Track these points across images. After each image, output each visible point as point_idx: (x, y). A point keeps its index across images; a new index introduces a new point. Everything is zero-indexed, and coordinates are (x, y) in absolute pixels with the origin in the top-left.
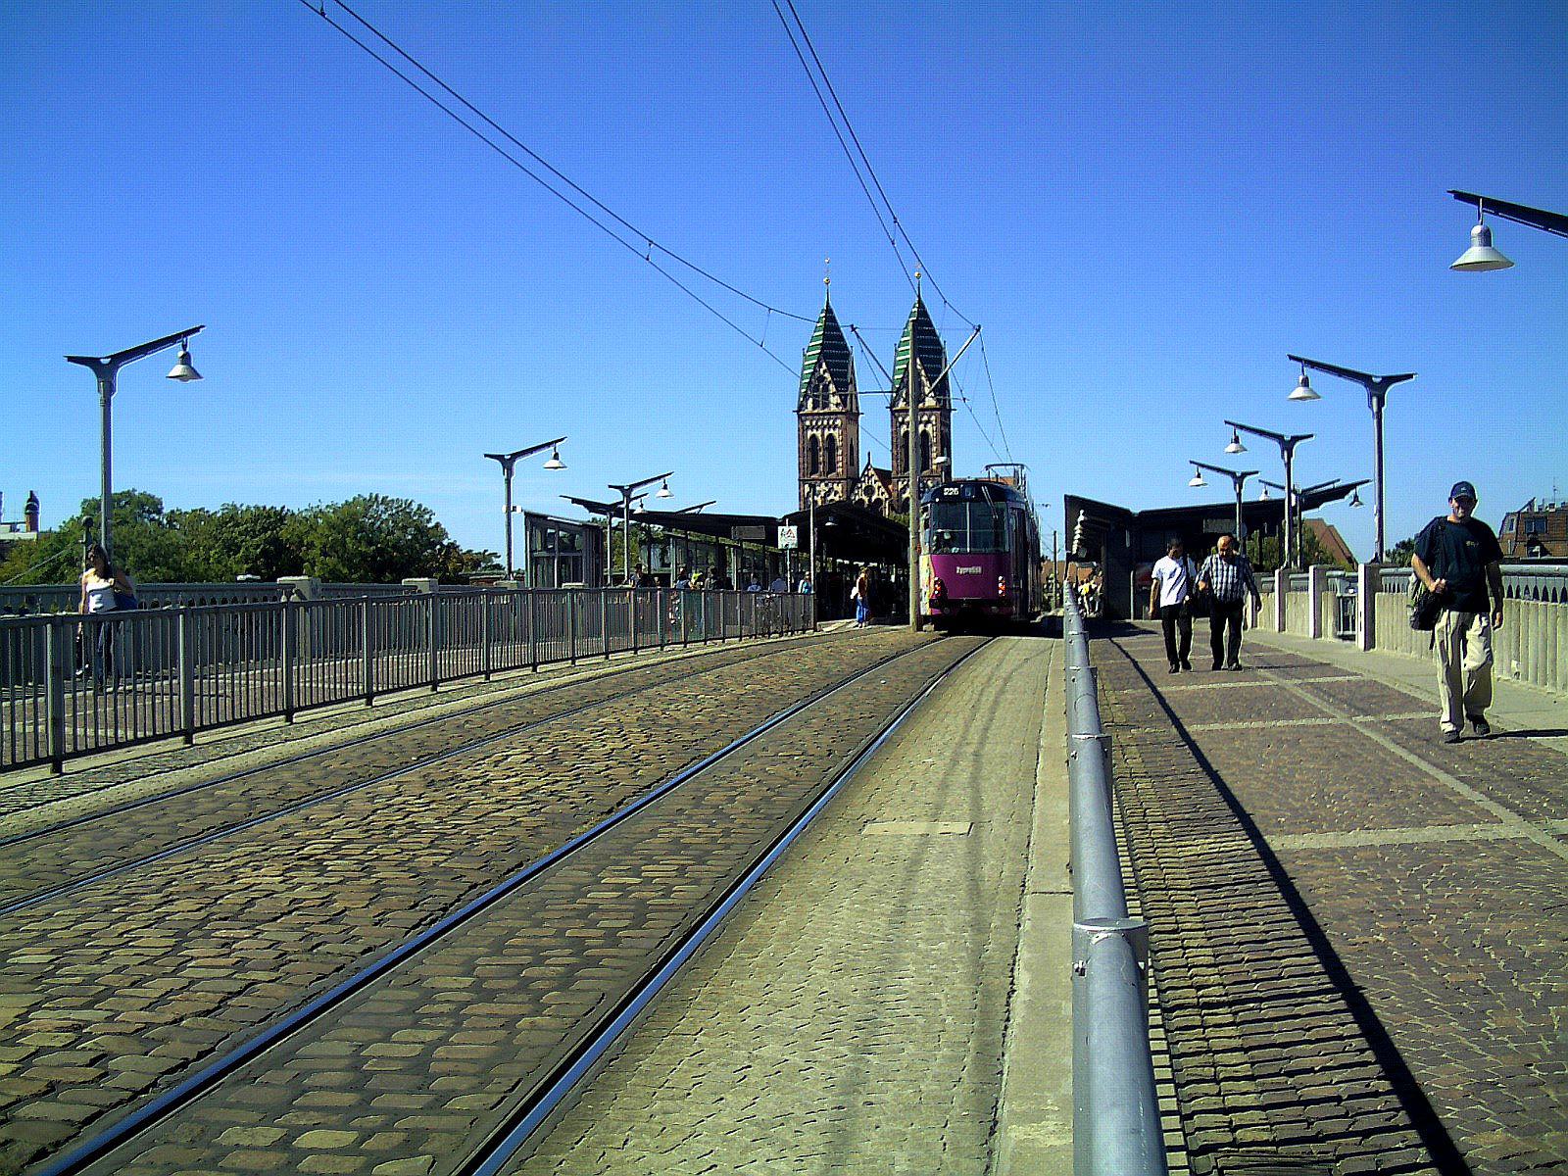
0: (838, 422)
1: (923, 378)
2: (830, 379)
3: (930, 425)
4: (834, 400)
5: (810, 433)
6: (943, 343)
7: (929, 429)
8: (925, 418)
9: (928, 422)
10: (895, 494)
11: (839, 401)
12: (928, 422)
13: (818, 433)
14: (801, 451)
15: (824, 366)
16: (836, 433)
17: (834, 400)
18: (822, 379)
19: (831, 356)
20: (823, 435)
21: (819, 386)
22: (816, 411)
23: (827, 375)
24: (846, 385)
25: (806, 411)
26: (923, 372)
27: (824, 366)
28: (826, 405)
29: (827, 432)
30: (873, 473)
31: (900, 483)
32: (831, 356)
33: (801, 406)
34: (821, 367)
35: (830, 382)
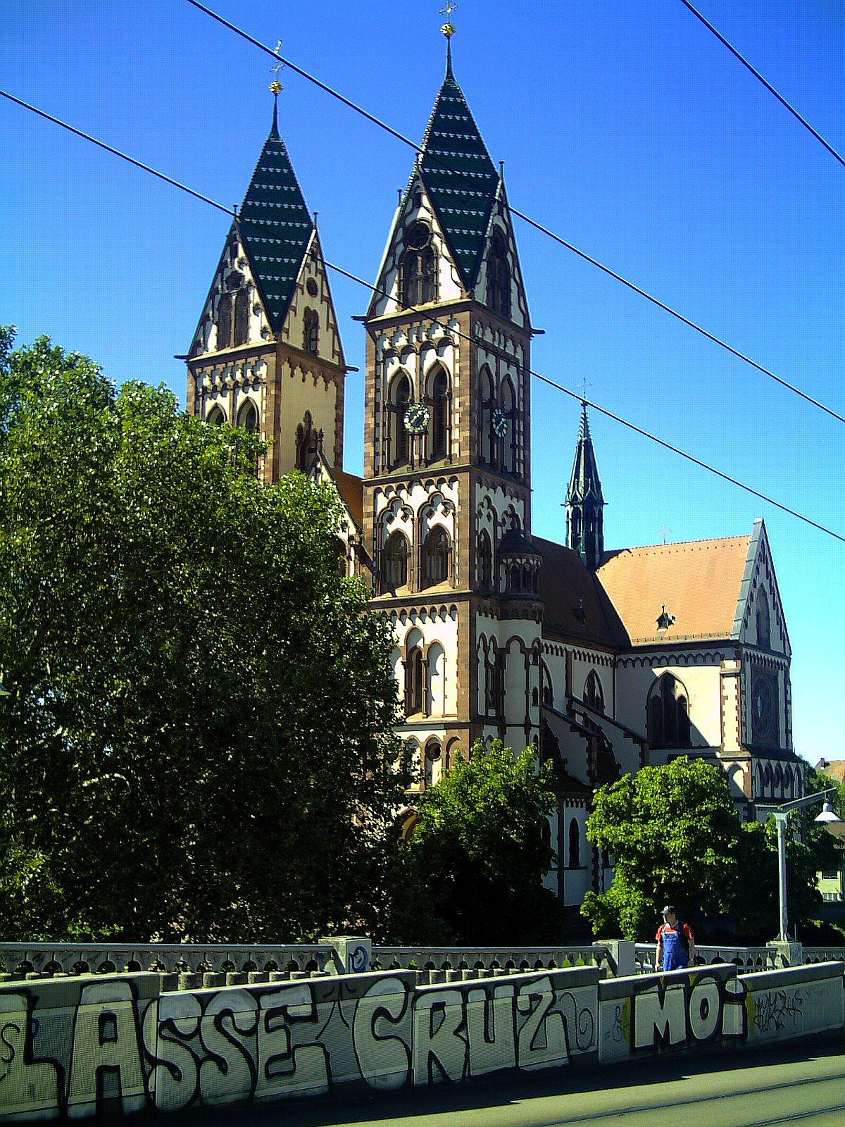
0: (263, 372)
3: (449, 349)
4: (257, 322)
6: (498, 171)
9: (445, 342)
10: (368, 523)
11: (265, 323)
12: (445, 342)
13: (224, 402)
15: (241, 253)
16: (257, 396)
17: (257, 322)
21: (228, 296)
25: (205, 355)
26: (436, 227)
27: (241, 253)
28: (242, 336)
29: (241, 397)
31: (380, 496)
33: (197, 345)
34: (234, 254)
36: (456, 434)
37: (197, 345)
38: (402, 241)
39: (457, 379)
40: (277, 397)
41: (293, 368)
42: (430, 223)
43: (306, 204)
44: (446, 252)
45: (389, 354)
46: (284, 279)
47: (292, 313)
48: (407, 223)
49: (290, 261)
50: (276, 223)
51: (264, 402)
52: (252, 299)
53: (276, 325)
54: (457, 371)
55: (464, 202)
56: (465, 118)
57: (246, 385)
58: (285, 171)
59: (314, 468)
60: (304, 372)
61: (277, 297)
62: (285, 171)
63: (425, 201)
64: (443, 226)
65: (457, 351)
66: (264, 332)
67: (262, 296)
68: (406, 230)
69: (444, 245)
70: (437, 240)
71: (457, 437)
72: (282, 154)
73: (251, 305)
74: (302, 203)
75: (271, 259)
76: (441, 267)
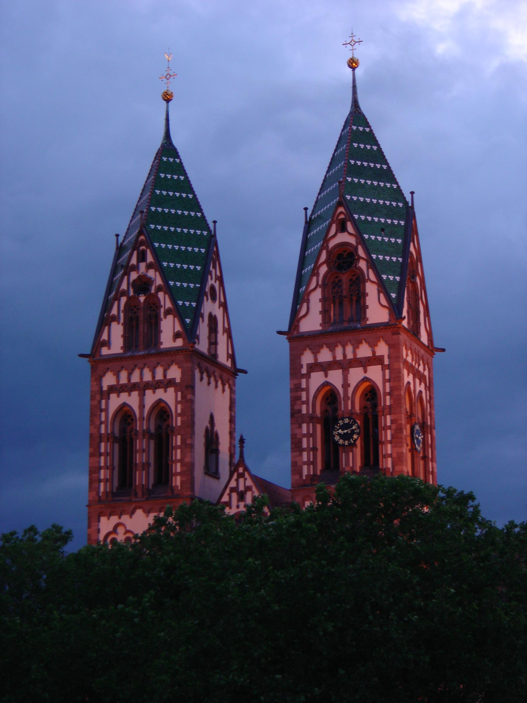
1: (362, 264)
2: (159, 281)
5: (115, 402)
6: (408, 198)
7: (375, 373)
8: (364, 351)
9: (376, 360)
11: (178, 328)
13: (132, 400)
14: (95, 439)
15: (150, 258)
16: (169, 396)
17: (169, 326)
18: (143, 285)
19: (166, 237)
20: (142, 406)
22: (129, 354)
23: (151, 273)
24: (199, 296)
26: (361, 252)
27: (150, 258)
29: (151, 398)
30: (249, 483)
32: (166, 237)
33: (99, 343)
34: (142, 257)
35: (159, 289)
36: (389, 449)
37: (99, 343)
38: (326, 262)
39: (388, 397)
40: (192, 402)
41: (202, 373)
42: (356, 249)
43: (204, 211)
44: (372, 277)
45: (314, 367)
46: (192, 286)
47: (201, 319)
48: (332, 244)
49: (195, 268)
50: (179, 230)
51: (179, 406)
52: (162, 303)
53: (189, 333)
54: (388, 390)
55: (382, 229)
56: (375, 148)
57: (155, 385)
58: (182, 178)
59: (236, 474)
60: (209, 377)
61: (187, 304)
62: (182, 178)
63: (350, 227)
64: (368, 252)
65: (387, 372)
66: (177, 336)
67: (174, 301)
68: (329, 253)
69: (370, 270)
70: (362, 264)
71: (389, 452)
72: (178, 161)
73: (162, 310)
74: (201, 210)
75: (179, 266)
76: (367, 291)
